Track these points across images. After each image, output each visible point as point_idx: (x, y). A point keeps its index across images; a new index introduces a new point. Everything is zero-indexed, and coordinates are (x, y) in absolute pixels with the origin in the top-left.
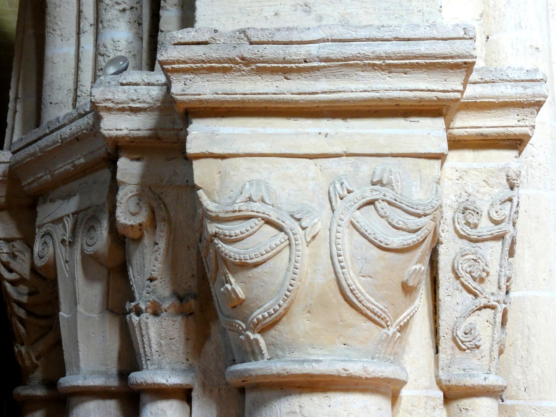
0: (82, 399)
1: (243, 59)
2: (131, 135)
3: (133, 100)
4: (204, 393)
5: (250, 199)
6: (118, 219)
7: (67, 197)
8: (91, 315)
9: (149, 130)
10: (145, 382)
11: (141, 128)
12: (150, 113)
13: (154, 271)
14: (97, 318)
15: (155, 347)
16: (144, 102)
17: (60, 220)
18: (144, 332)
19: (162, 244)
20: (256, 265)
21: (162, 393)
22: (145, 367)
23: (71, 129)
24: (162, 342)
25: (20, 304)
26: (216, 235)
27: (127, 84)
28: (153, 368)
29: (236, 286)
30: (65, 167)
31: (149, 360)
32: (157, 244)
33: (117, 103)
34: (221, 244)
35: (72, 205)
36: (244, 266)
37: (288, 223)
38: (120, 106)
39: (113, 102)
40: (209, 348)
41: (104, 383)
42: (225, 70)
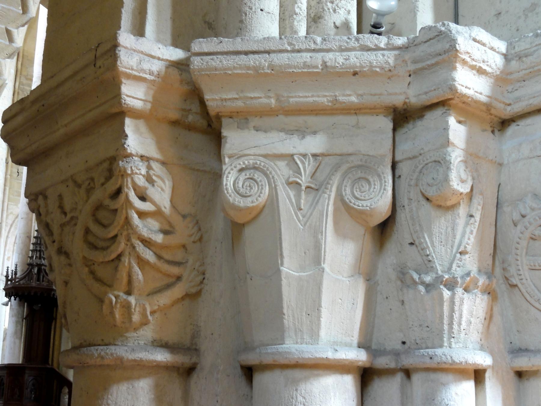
0: (316, 372)
2: (474, 97)
3: (484, 62)
4: (493, 374)
6: (451, 183)
7: (302, 132)
8: (337, 277)
9: (488, 97)
10: (466, 362)
11: (482, 91)
12: (488, 78)
13: (468, 245)
14: (348, 282)
15: (464, 325)
16: (490, 67)
17: (290, 158)
18: (456, 308)
19: (478, 217)
21: (461, 372)
22: (446, 344)
23: (346, 59)
24: (472, 319)
25: (147, 243)
27: (478, 42)
28: (457, 346)
30: (314, 99)
31: (454, 337)
32: (472, 216)
33: (473, 59)
35: (314, 144)
38: (474, 63)
39: (470, 57)
41: (356, 357)
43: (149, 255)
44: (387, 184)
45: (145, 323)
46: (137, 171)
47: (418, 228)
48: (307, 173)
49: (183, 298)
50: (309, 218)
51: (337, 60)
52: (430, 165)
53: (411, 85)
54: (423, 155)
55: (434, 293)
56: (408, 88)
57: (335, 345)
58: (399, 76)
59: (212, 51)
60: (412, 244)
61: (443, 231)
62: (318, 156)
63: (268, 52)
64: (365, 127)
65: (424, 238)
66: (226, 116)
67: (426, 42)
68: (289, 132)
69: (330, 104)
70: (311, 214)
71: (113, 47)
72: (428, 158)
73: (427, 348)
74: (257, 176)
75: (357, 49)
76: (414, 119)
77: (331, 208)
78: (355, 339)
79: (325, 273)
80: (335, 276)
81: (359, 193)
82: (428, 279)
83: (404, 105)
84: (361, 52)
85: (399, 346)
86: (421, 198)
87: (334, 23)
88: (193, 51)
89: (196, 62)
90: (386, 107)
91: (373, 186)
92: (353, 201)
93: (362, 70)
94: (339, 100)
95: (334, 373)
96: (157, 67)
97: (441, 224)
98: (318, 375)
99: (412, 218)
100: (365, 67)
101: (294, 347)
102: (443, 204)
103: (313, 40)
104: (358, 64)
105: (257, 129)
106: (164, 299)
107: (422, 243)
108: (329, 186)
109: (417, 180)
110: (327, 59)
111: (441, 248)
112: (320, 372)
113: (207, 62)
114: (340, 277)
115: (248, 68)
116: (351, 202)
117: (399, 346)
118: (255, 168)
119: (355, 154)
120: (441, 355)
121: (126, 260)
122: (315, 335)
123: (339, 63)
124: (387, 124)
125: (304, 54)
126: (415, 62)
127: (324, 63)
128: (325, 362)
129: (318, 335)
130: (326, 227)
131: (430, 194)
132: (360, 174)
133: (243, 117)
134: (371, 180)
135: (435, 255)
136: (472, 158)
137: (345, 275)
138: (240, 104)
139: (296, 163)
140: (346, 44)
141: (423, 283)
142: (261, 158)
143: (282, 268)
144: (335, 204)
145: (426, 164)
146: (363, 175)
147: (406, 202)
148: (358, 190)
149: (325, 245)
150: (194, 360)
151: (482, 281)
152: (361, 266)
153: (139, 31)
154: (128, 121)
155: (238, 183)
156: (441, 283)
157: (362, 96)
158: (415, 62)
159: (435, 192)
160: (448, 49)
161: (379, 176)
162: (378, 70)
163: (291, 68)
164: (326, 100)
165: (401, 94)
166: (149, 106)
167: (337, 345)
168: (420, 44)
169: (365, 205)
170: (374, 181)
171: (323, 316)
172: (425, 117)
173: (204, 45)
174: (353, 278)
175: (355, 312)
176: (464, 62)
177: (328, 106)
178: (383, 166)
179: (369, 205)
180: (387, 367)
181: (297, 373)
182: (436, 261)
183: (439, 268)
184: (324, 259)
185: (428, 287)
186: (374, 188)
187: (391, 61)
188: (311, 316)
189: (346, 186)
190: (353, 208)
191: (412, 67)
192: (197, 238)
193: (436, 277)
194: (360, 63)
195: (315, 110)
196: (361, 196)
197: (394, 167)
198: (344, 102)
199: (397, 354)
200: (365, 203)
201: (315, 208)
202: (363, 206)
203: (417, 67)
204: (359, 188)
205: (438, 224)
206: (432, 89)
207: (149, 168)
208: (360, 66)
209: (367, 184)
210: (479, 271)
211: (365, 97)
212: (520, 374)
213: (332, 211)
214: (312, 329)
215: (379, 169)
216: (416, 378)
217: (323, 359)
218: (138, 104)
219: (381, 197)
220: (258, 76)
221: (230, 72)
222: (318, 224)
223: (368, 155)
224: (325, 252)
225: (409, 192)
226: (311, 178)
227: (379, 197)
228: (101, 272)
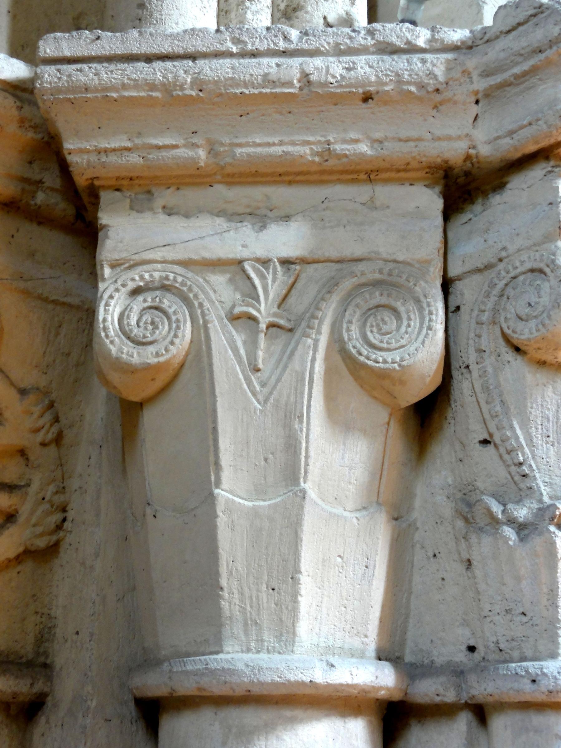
0: (288, 713)
7: (260, 217)
8: (334, 510)
14: (355, 521)
23: (348, 69)
35: (285, 239)
41: (373, 679)
44: (434, 317)
47: (498, 408)
48: (271, 297)
49: (19, 559)
50: (274, 387)
51: (331, 71)
52: (521, 278)
53: (479, 121)
54: (505, 261)
55: (537, 542)
56: (474, 127)
57: (329, 654)
58: (455, 103)
59: (79, 54)
60: (485, 442)
61: (551, 414)
62: (293, 263)
63: (193, 57)
64: (388, 207)
65: (512, 427)
66: (109, 187)
67: (509, 32)
68: (235, 216)
69: (317, 159)
70: (278, 380)
72: (518, 264)
73: (524, 659)
74: (169, 302)
75: (371, 49)
76: (485, 194)
77: (319, 367)
79: (307, 500)
80: (328, 508)
81: (378, 336)
82: (522, 513)
83: (465, 161)
84: (379, 57)
86: (504, 348)
87: (325, 18)
88: (41, 54)
90: (429, 167)
91: (405, 323)
92: (365, 352)
93: (380, 89)
94: (335, 150)
95: (327, 715)
98: (293, 721)
99: (486, 389)
100: (386, 84)
101: (241, 659)
102: (549, 358)
103: (283, 34)
104: (373, 79)
105: (169, 211)
107: (508, 439)
108: (316, 322)
109: (495, 311)
110: (310, 69)
111: (548, 449)
112: (298, 713)
113: (69, 76)
114: (339, 511)
115: (152, 87)
116: (360, 354)
118: (165, 288)
119: (368, 259)
120: (555, 673)
122: (286, 633)
123: (334, 77)
124: (432, 201)
125: (265, 61)
126: (486, 74)
128: (308, 691)
129: (294, 634)
130: (309, 406)
131: (523, 337)
132: (378, 299)
133: (144, 187)
134: (402, 309)
135: (536, 462)
137: (350, 505)
139: (249, 278)
140: (348, 41)
141: (511, 522)
142: (178, 269)
143: (217, 491)
144: (327, 358)
145: (514, 278)
146: (384, 300)
147: (472, 357)
148: (375, 330)
149: (307, 442)
150: (39, 687)
152: (382, 488)
155: (128, 317)
156: (552, 519)
157: (381, 142)
158: (486, 74)
159: (534, 331)
160: (557, 38)
161: (418, 301)
162: (413, 89)
163: (238, 86)
164: (308, 151)
165: (459, 138)
167: (334, 654)
168: (497, 37)
169: (390, 360)
170: (408, 312)
171: (303, 592)
172: (509, 186)
173: (64, 44)
174: (365, 513)
175: (370, 584)
177: (313, 162)
178: (426, 282)
179: (398, 359)
180: (438, 699)
181: (249, 716)
182: (537, 475)
183: (545, 490)
184: (306, 472)
185: (522, 528)
186: (409, 326)
187: (440, 72)
188: (278, 593)
189: (350, 322)
190: (364, 366)
191: (480, 85)
192: (50, 436)
193: (539, 509)
194: (377, 76)
195: (287, 174)
196: (382, 342)
197: (447, 286)
198: (346, 156)
199: (458, 673)
200: (389, 356)
201: (286, 367)
202: (385, 362)
203: (492, 83)
204: (378, 325)
205: (539, 400)
206: (525, 122)
208: (376, 82)
209: (393, 317)
211: (386, 144)
213: (322, 373)
214: (281, 620)
215: (417, 288)
216: (500, 724)
217: (303, 683)
219: (423, 343)
220: (172, 103)
221: (115, 95)
222: (292, 399)
223: (395, 261)
224: (307, 457)
225: (479, 336)
226: (279, 306)
227: (418, 344)
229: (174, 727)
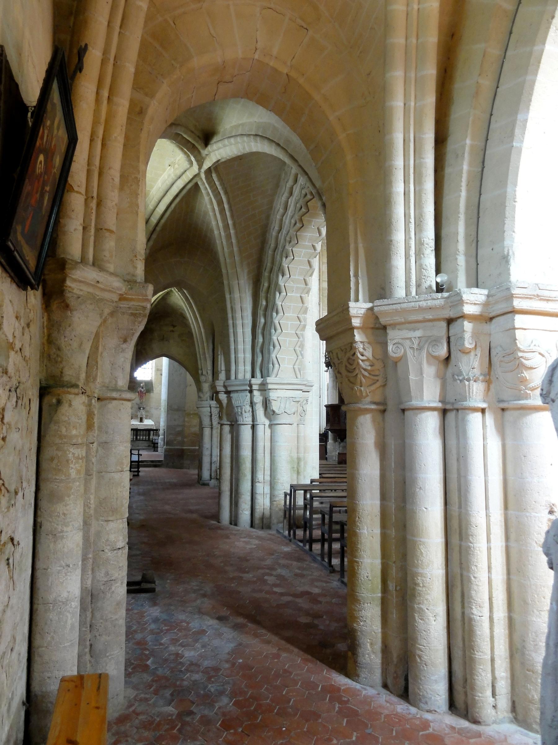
1: (537, 295)
5: (535, 345)
7: (414, 330)
15: (474, 393)
19: (479, 355)
20: (535, 368)
21: (475, 410)
26: (521, 357)
29: (526, 374)
34: (523, 360)
35: (418, 333)
36: (531, 368)
37: (546, 355)
40: (490, 393)
42: (531, 298)
43: (366, 374)
45: (367, 396)
46: (360, 347)
49: (380, 387)
57: (429, 402)
63: (400, 303)
68: (410, 330)
71: (347, 308)
74: (399, 346)
77: (425, 356)
78: (437, 399)
82: (461, 378)
85: (454, 401)
89: (376, 309)
96: (363, 311)
97: (465, 358)
101: (415, 403)
105: (399, 329)
106: (373, 388)
115: (393, 310)
117: (454, 401)
118: (399, 343)
121: (359, 376)
122: (422, 399)
124: (444, 324)
127: (419, 306)
133: (394, 326)
136: (475, 335)
138: (392, 322)
141: (459, 379)
151: (481, 378)
153: (357, 300)
154: (355, 330)
158: (451, 302)
166: (362, 325)
176: (467, 303)
181: (417, 411)
185: (461, 381)
187: (443, 303)
191: (450, 304)
199: (453, 404)
207: (364, 345)
210: (481, 374)
212: (503, 410)
216: (460, 411)
218: (358, 325)
220: (397, 311)
228: (352, 379)
229: (406, 413)
